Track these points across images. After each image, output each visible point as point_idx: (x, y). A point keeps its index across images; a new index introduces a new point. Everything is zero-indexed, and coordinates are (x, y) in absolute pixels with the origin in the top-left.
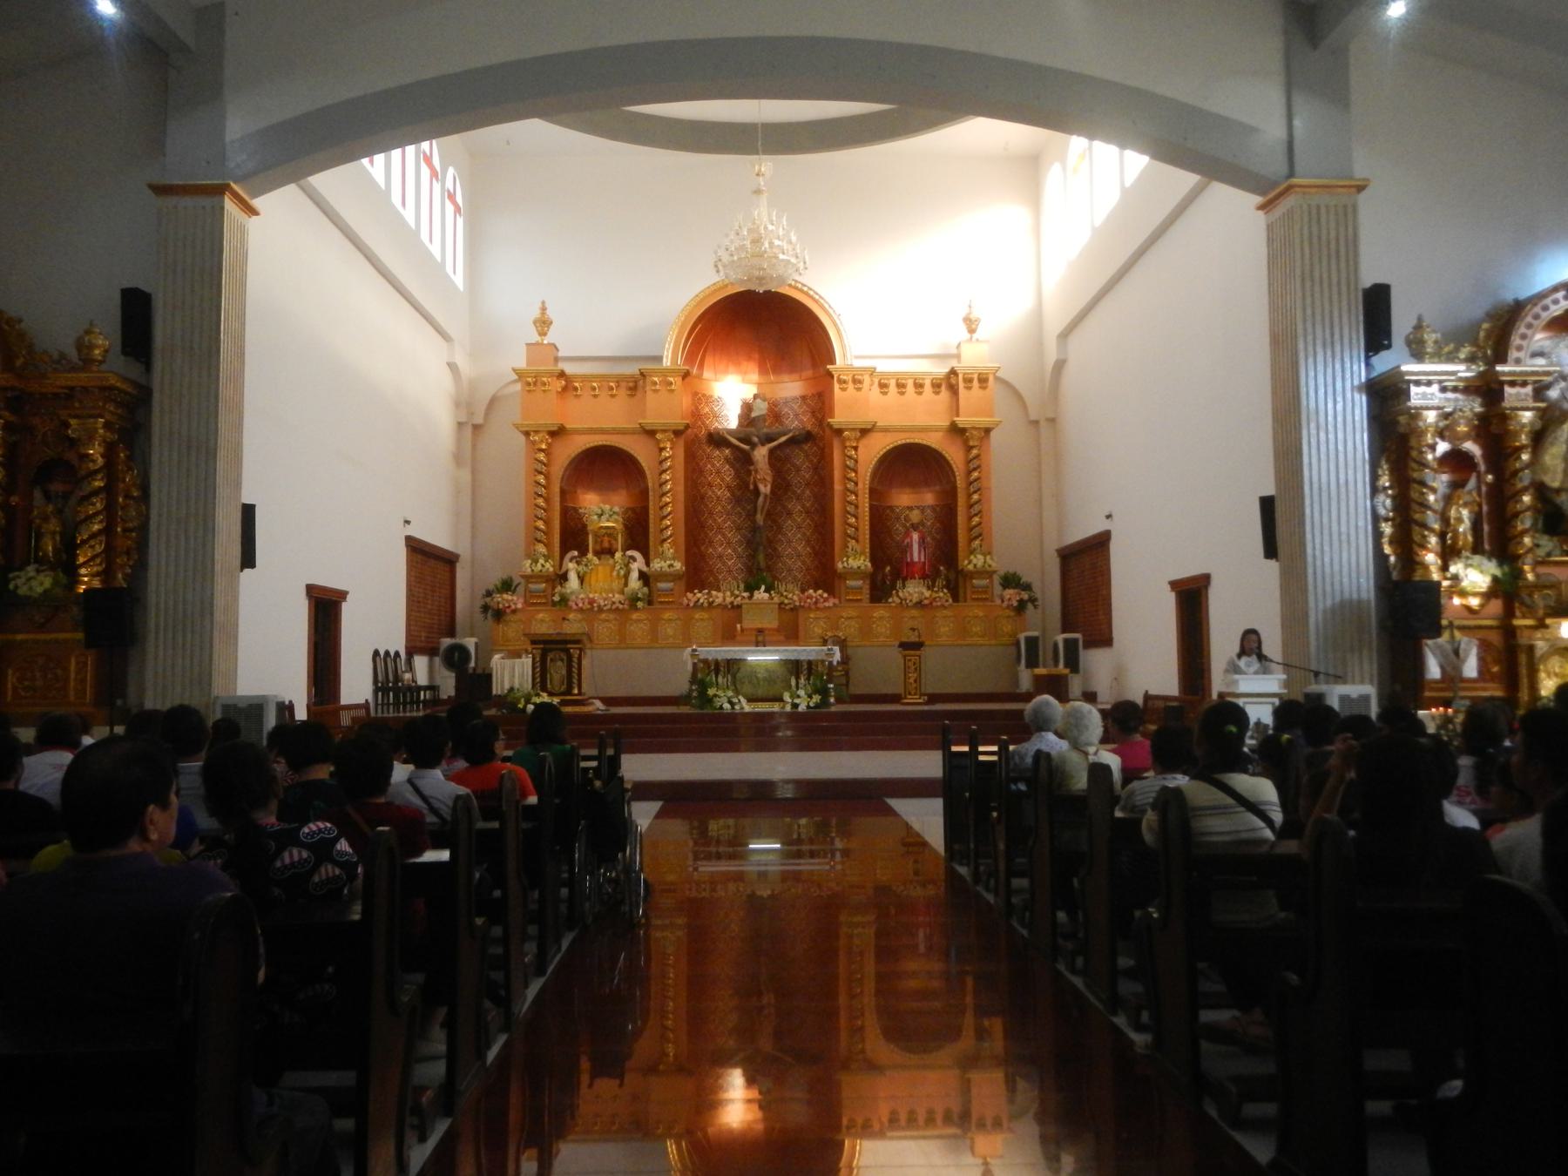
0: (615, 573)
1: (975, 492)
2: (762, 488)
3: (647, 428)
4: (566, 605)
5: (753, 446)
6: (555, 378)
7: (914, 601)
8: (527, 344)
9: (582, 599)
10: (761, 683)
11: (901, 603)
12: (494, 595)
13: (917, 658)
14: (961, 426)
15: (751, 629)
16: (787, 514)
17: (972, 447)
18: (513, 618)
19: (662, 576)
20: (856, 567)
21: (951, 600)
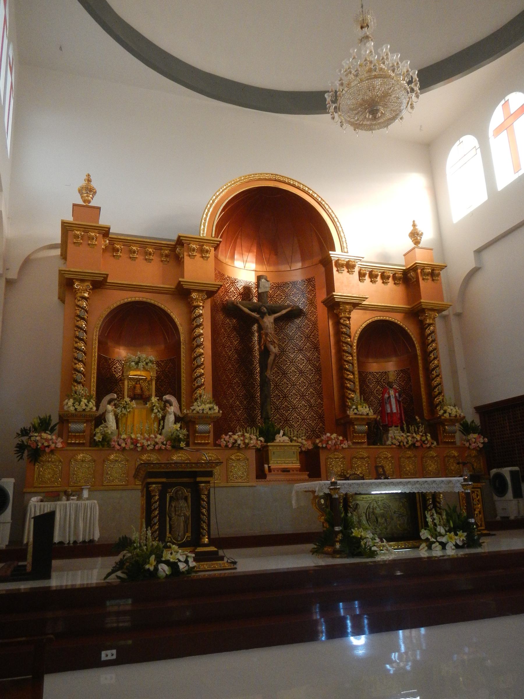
0: (153, 416)
1: (435, 358)
2: (272, 347)
3: (185, 287)
4: (109, 445)
5: (263, 315)
6: (102, 235)
7: (410, 443)
8: (74, 205)
9: (124, 439)
10: (379, 520)
11: (399, 445)
12: (31, 434)
13: (479, 490)
14: (424, 307)
15: (278, 470)
16: (283, 374)
17: (430, 325)
18: (54, 457)
19: (203, 418)
20: (365, 413)
21: (435, 443)
